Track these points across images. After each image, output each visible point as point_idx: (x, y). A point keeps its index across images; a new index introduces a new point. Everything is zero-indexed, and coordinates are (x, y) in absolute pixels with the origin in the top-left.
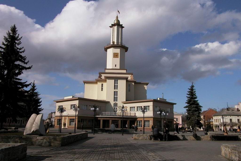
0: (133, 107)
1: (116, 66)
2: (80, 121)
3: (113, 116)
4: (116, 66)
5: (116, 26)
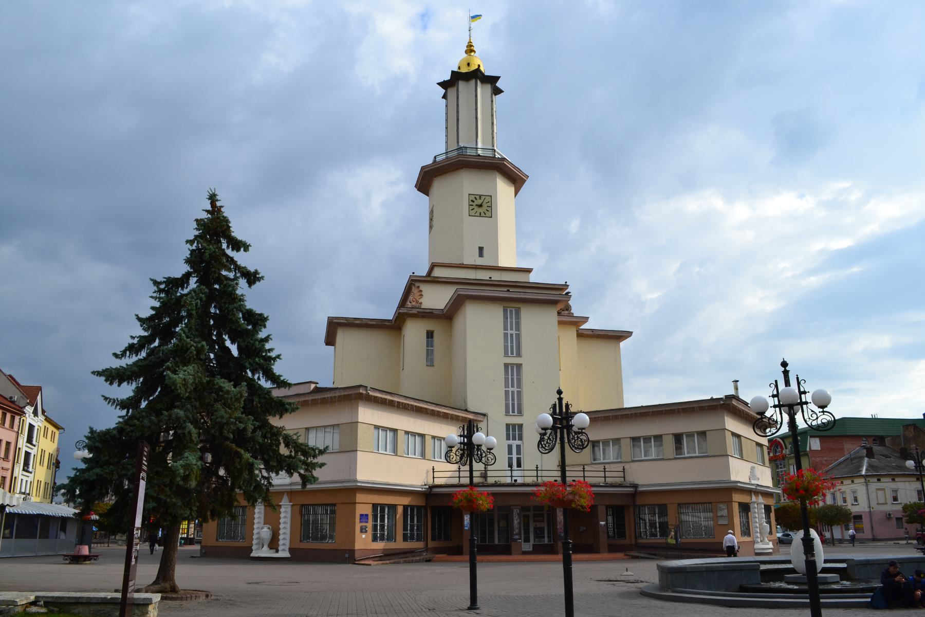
1: (481, 255)
2: (367, 515)
3: (841, 463)
4: (481, 255)
5: (473, 81)
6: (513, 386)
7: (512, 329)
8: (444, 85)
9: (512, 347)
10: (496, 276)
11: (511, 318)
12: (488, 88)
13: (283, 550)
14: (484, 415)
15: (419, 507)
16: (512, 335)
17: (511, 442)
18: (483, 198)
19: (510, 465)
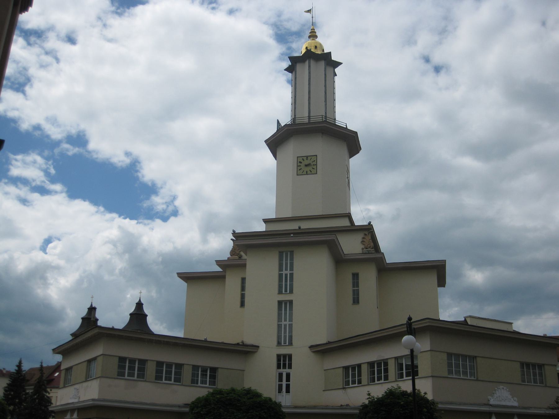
0: (353, 368)
5: (307, 62)
8: (290, 69)
11: (286, 260)
12: (322, 64)
14: (258, 347)
16: (286, 275)
17: (281, 370)
18: (309, 158)
19: (280, 390)
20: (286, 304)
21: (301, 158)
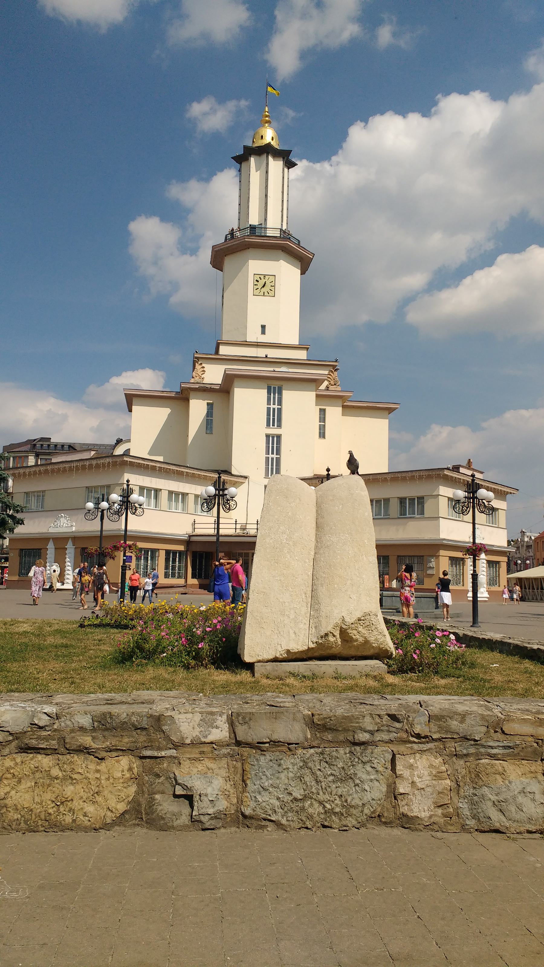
1: (263, 332)
4: (263, 332)
6: (273, 453)
7: (274, 404)
9: (274, 419)
10: (273, 353)
13: (67, 583)
14: (246, 478)
15: (180, 552)
16: (274, 409)
18: (267, 277)
20: (273, 438)
21: (258, 276)
